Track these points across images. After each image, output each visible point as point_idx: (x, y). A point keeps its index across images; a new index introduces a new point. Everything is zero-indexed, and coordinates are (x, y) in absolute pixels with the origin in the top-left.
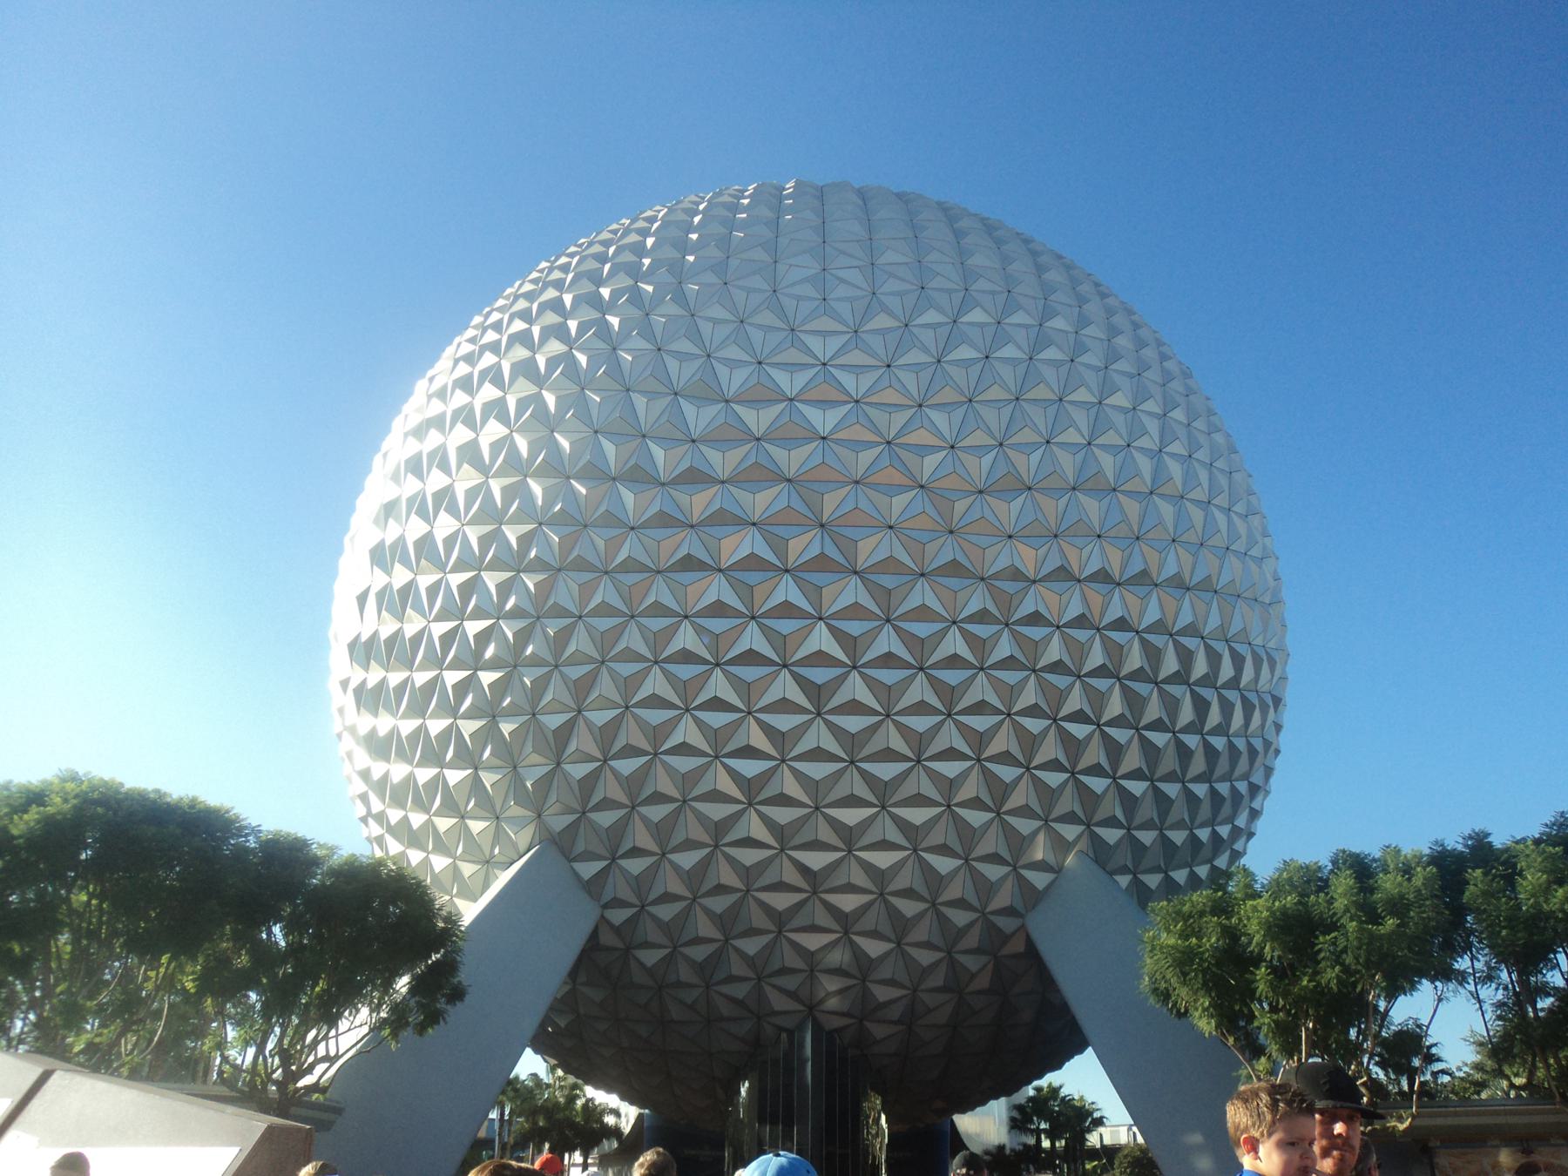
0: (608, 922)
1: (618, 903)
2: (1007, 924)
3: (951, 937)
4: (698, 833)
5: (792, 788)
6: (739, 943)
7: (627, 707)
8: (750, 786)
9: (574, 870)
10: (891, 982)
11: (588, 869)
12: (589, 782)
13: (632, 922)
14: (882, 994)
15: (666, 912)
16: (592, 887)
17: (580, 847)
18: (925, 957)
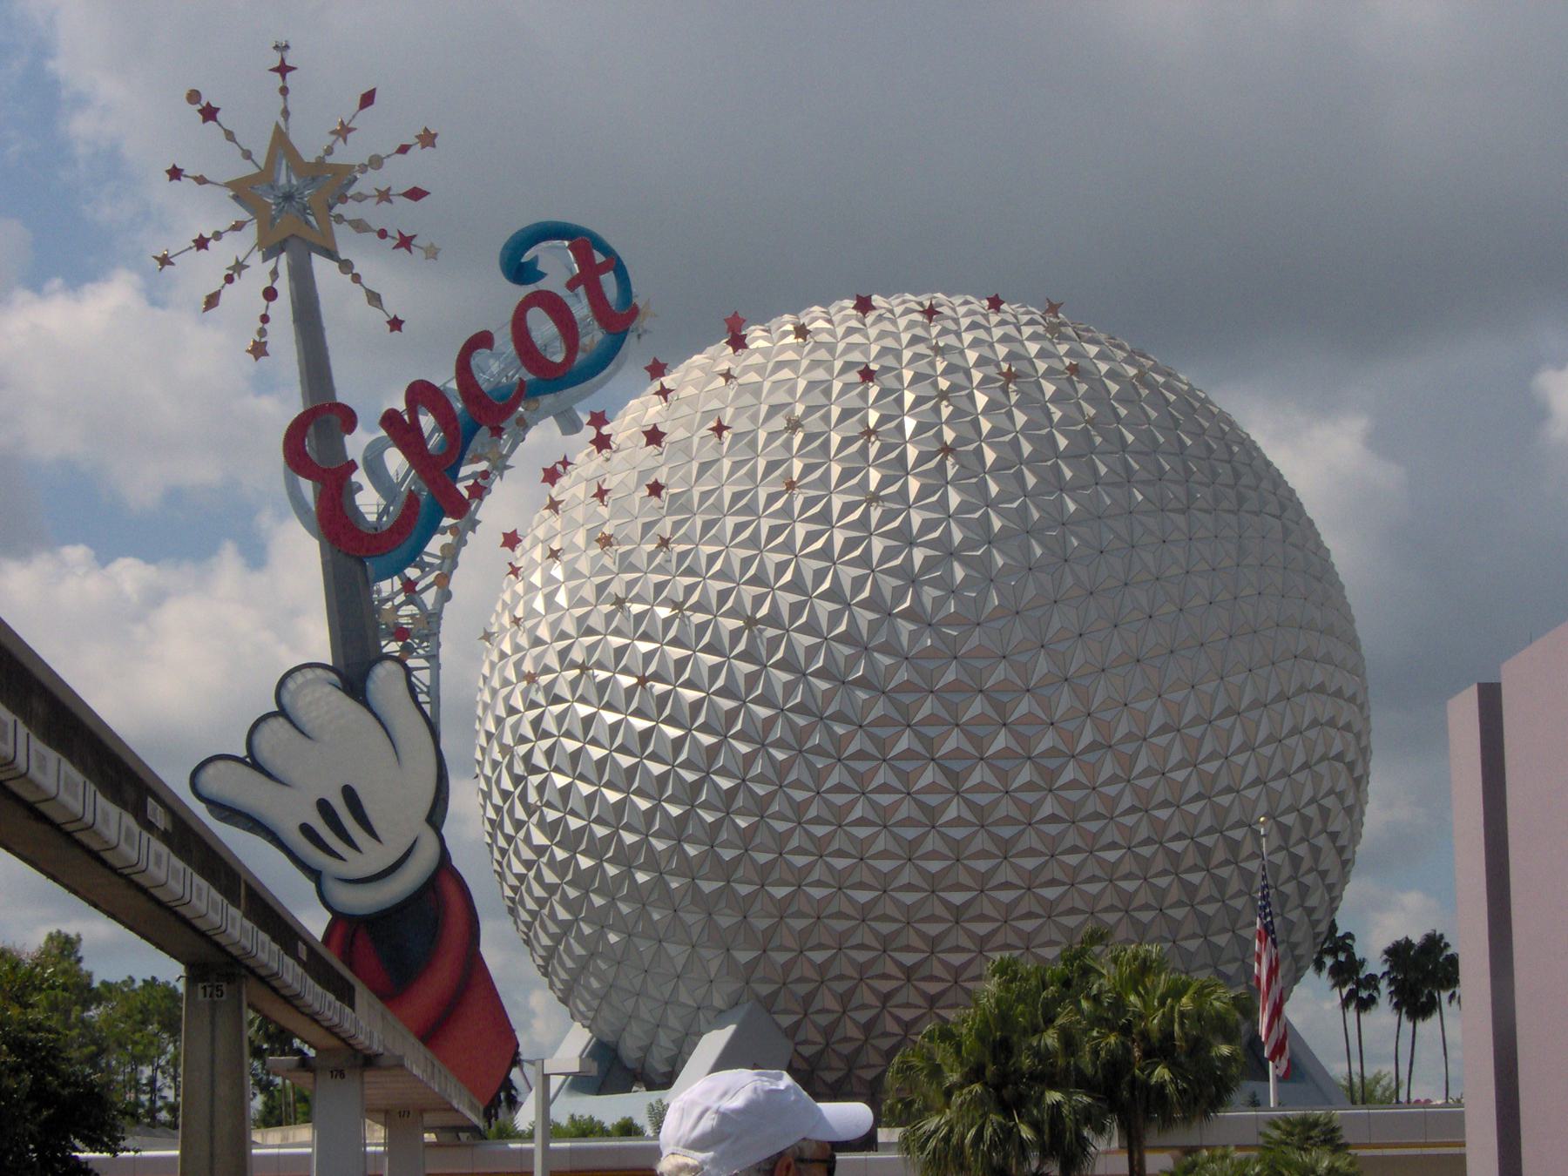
0: (800, 1055)
4: (870, 999)
5: (938, 970)
8: (909, 972)
9: (774, 1020)
11: (786, 1021)
12: (788, 967)
16: (791, 1032)
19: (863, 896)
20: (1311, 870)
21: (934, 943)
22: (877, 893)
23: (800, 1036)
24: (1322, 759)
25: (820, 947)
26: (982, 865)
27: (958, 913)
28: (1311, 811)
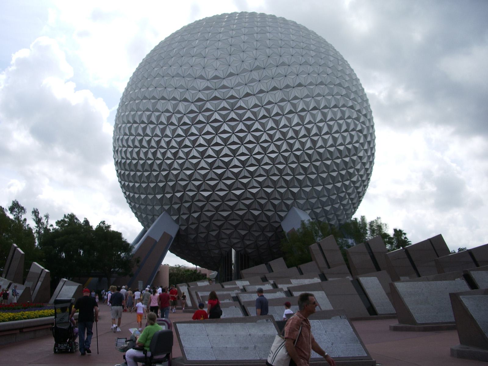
1: (181, 225)
2: (276, 225)
3: (263, 229)
6: (211, 233)
7: (177, 181)
10: (249, 240)
11: (175, 218)
13: (187, 229)
14: (248, 243)
15: (193, 227)
16: (177, 221)
17: (172, 213)
18: (257, 234)
19: (188, 172)
20: (351, 168)
21: (213, 188)
22: (194, 171)
23: (180, 223)
24: (353, 130)
25: (179, 191)
26: (226, 159)
27: (220, 176)
28: (350, 146)
